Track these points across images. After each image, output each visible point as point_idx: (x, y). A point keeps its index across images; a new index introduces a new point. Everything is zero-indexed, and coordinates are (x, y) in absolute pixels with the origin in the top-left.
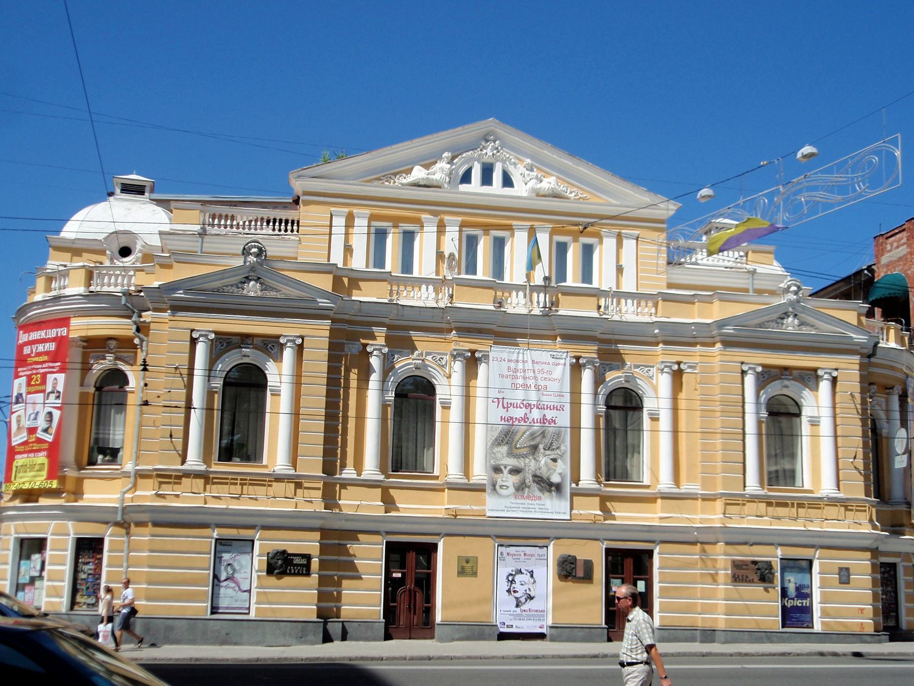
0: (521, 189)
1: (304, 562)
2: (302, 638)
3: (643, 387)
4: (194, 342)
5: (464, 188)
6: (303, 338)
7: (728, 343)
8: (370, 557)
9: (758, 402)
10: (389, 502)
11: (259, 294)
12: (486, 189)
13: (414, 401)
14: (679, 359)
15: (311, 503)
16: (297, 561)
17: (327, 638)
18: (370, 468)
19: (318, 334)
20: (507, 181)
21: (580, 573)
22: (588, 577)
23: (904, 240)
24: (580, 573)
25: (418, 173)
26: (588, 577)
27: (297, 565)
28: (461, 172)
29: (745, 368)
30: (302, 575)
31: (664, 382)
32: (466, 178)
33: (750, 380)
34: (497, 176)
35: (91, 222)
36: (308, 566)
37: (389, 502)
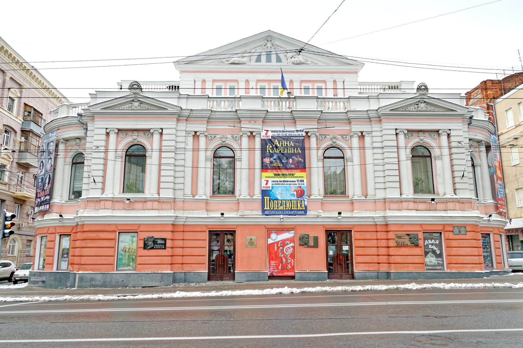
1: (163, 242)
4: (108, 134)
6: (162, 129)
11: (139, 108)
14: (362, 130)
16: (159, 242)
20: (279, 60)
21: (311, 243)
22: (316, 246)
23: (480, 92)
24: (311, 243)
27: (160, 244)
30: (162, 249)
31: (355, 141)
32: (258, 60)
33: (401, 137)
34: (274, 57)
36: (165, 244)
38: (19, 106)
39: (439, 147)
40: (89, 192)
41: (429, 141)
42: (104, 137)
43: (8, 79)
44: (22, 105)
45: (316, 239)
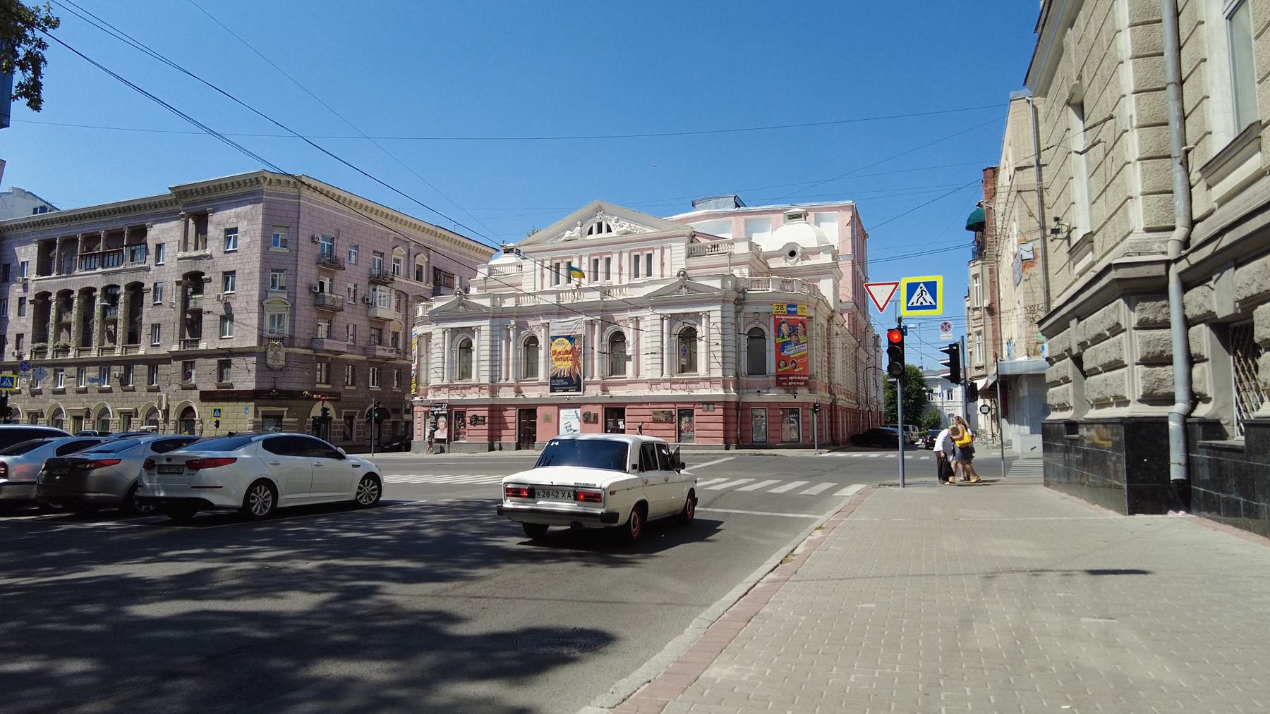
2: (481, 450)
3: (625, 330)
5: (590, 237)
7: (654, 306)
8: (511, 417)
9: (670, 335)
10: (518, 392)
15: (486, 395)
17: (491, 449)
18: (511, 381)
19: (485, 325)
20: (609, 230)
22: (596, 421)
25: (568, 234)
26: (596, 421)
32: (590, 232)
37: (518, 392)
38: (428, 271)
45: (596, 416)
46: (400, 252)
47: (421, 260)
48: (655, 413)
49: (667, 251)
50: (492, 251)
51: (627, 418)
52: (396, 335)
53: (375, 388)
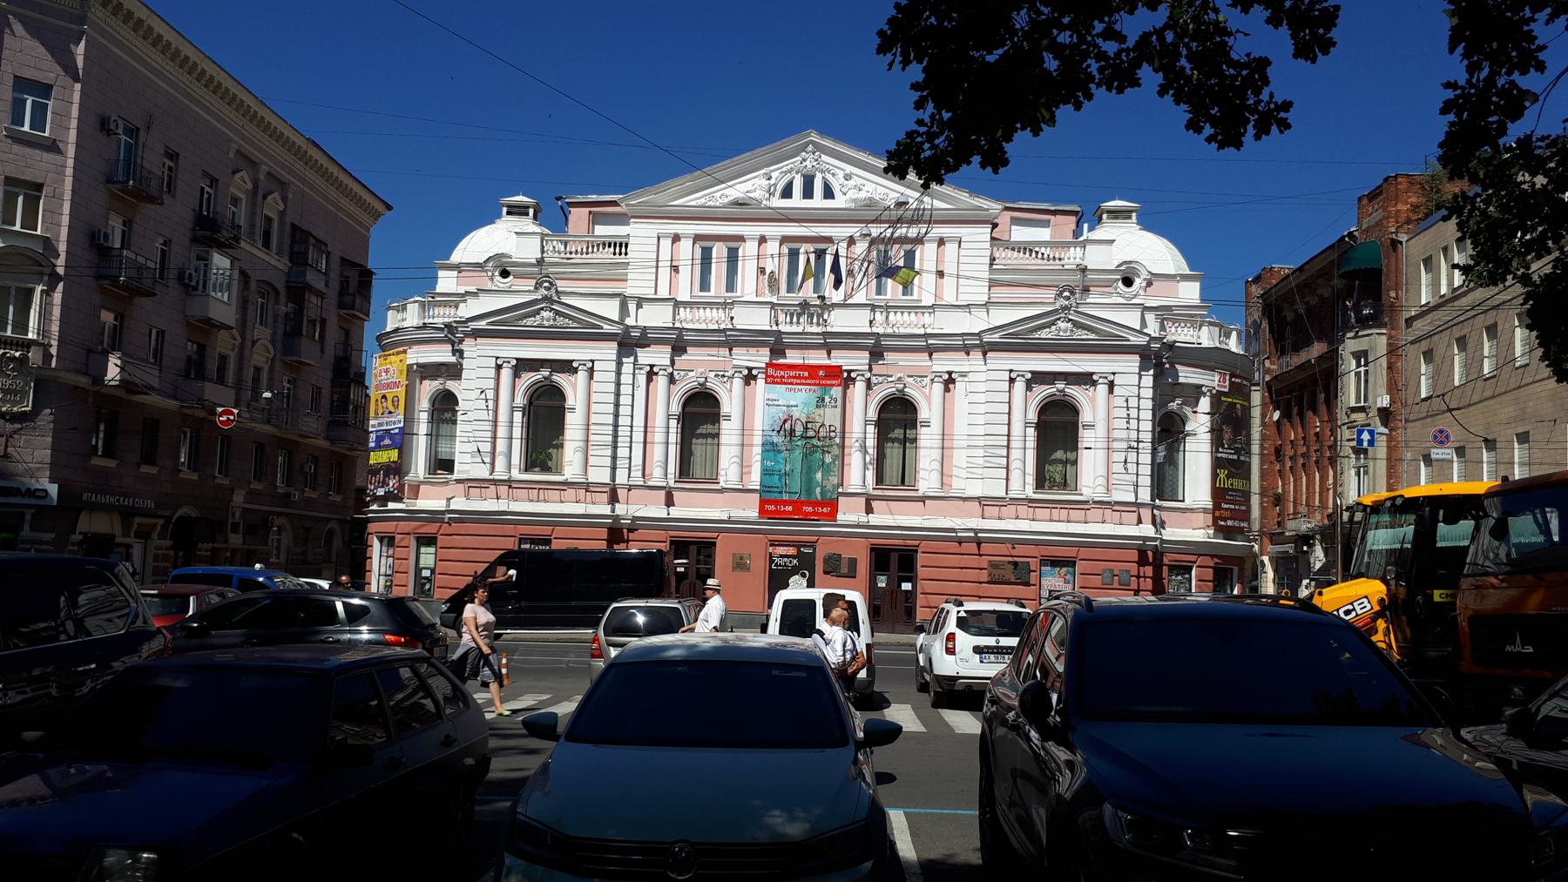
0: (840, 202)
4: (499, 367)
12: (808, 203)
13: (700, 412)
20: (829, 193)
21: (845, 570)
28: (780, 187)
29: (1013, 375)
32: (787, 193)
35: (478, 245)
38: (281, 231)
39: (1092, 406)
40: (467, 465)
41: (1075, 391)
42: (492, 373)
43: (262, 177)
44: (288, 229)
45: (853, 563)
46: (240, 185)
47: (272, 206)
48: (994, 565)
49: (951, 248)
50: (380, 208)
51: (921, 572)
52: (223, 359)
53: (188, 475)
